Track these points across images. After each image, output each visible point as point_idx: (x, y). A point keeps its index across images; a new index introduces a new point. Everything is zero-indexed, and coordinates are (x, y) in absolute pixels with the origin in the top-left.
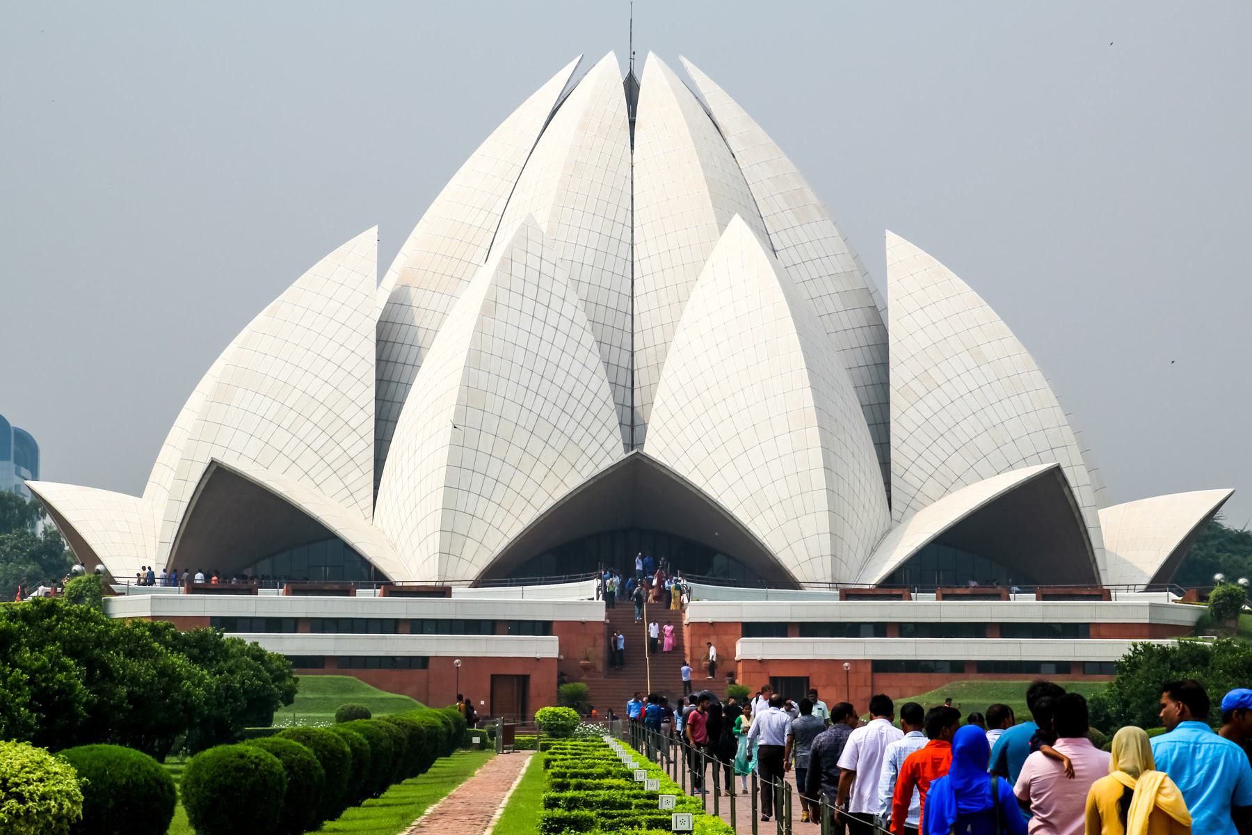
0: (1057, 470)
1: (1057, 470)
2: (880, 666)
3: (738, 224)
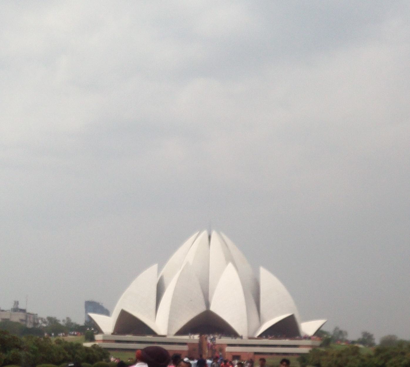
2: (256, 353)
3: (230, 265)
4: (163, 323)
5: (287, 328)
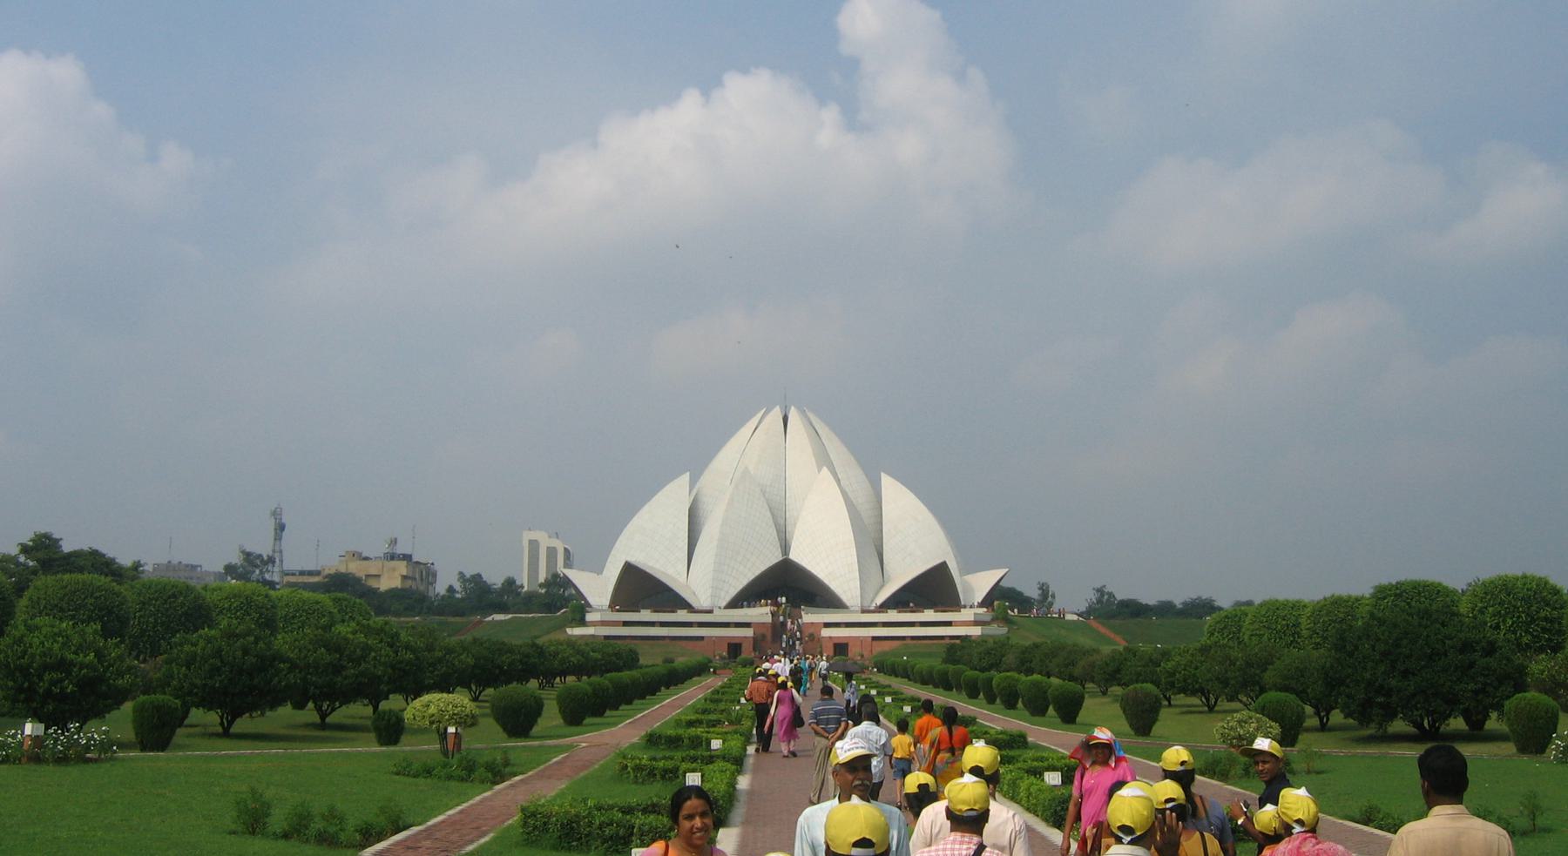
0: (943, 565)
1: (943, 565)
4: (709, 582)
5: (932, 589)
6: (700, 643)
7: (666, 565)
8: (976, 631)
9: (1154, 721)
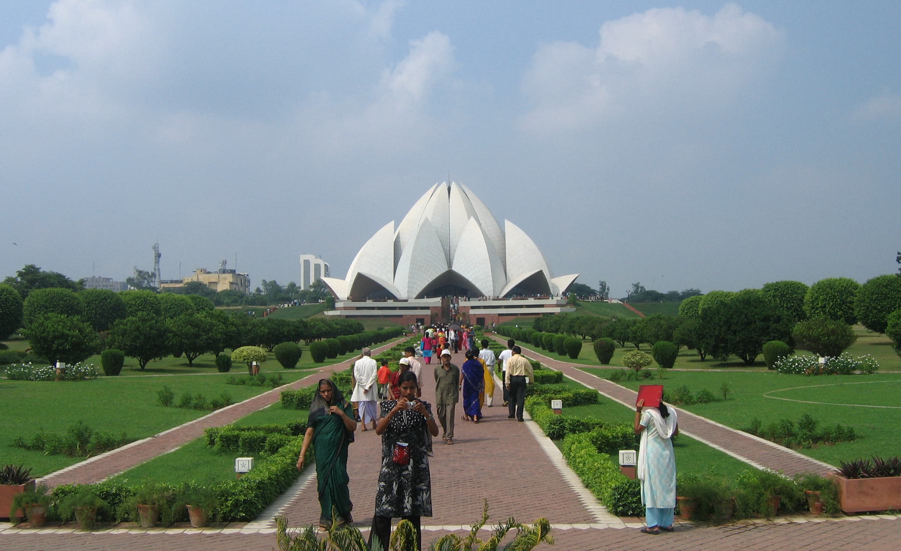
4: (405, 284)
5: (535, 285)
6: (400, 319)
7: (381, 275)
8: (557, 310)
9: (611, 356)
